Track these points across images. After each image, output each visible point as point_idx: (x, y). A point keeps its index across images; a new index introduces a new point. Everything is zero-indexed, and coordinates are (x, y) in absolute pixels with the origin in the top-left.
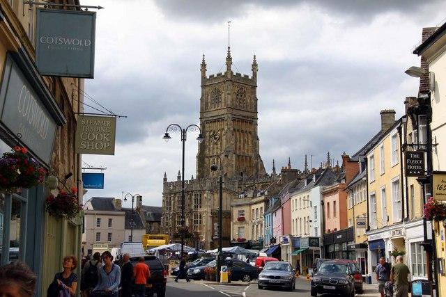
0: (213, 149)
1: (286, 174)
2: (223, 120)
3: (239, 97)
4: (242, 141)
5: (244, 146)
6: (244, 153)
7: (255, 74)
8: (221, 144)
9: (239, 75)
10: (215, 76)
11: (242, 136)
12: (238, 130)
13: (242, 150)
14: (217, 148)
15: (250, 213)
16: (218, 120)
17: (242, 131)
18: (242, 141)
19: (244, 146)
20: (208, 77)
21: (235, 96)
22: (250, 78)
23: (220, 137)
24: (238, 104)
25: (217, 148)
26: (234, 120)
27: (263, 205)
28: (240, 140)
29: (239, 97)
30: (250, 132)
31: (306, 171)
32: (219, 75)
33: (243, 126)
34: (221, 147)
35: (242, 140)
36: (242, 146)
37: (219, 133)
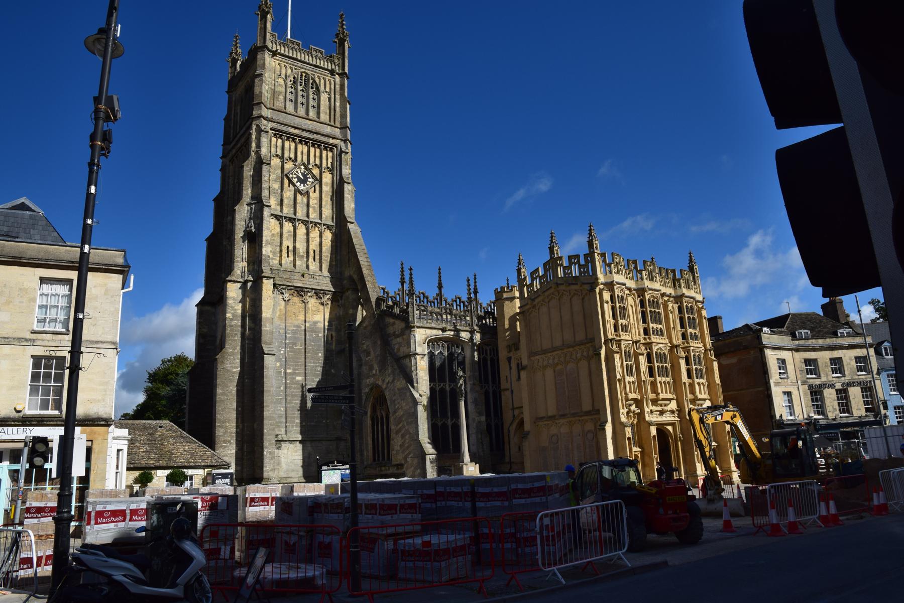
16: (316, 144)
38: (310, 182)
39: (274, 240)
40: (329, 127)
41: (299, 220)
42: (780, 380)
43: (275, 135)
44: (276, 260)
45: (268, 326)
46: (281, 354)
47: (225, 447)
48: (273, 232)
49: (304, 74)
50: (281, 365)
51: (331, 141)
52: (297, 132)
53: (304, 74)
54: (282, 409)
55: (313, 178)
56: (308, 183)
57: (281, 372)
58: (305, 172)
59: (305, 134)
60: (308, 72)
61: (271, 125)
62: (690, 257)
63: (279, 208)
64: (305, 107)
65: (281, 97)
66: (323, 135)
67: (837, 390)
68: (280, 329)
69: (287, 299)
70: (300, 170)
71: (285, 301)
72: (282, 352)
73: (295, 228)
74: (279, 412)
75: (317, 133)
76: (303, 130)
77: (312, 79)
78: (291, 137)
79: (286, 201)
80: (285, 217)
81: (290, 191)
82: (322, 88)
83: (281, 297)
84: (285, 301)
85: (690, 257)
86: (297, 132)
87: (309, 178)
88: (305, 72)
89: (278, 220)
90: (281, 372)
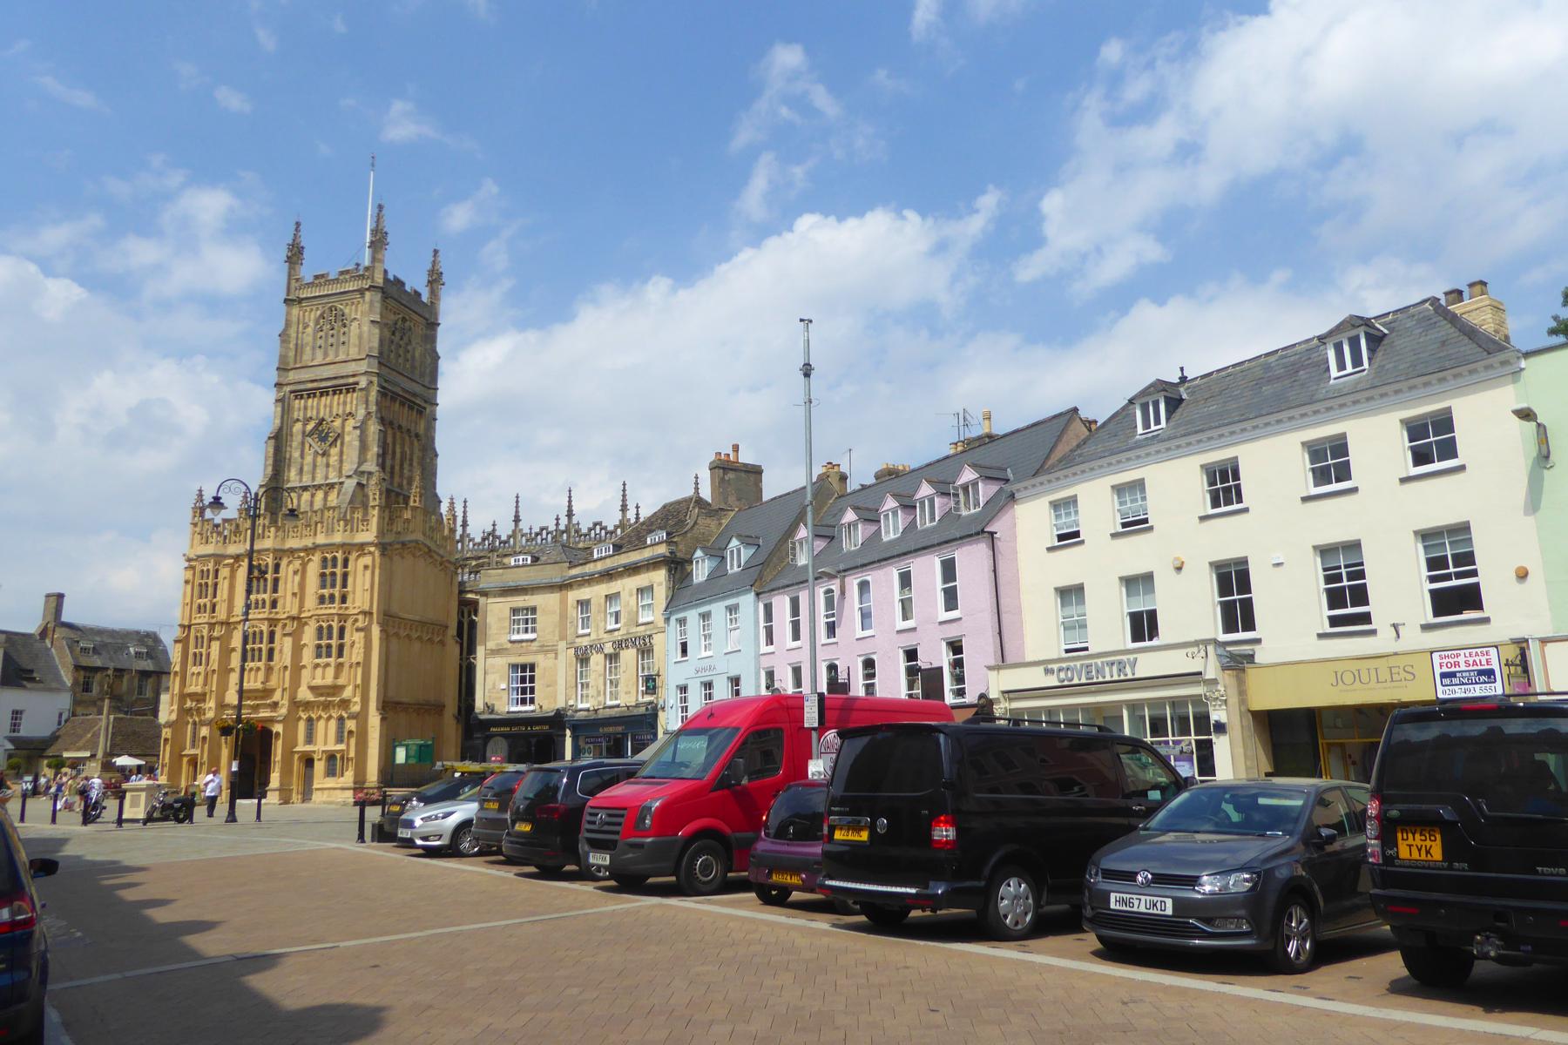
0: (315, 466)
1: (731, 475)
2: (351, 388)
3: (397, 338)
4: (398, 455)
5: (402, 466)
6: (400, 486)
7: (434, 294)
8: (341, 453)
9: (399, 283)
11: (398, 441)
12: (391, 423)
13: (397, 479)
14: (328, 465)
15: (563, 616)
16: (337, 390)
17: (400, 427)
18: (398, 455)
19: (402, 466)
20: (308, 279)
21: (387, 334)
22: (425, 298)
23: (339, 436)
24: (392, 355)
25: (328, 465)
26: (384, 393)
27: (659, 577)
28: (394, 453)
29: (397, 338)
30: (417, 436)
31: (622, 525)
33: (404, 417)
34: (341, 461)
35: (398, 450)
36: (397, 468)
37: (338, 423)
40: (354, 363)
41: (314, 486)
42: (509, 645)
43: (296, 397)
49: (333, 309)
51: (351, 380)
53: (333, 309)
56: (330, 439)
63: (298, 478)
64: (322, 350)
65: (308, 348)
66: (342, 377)
67: (606, 655)
73: (313, 496)
75: (335, 378)
76: (322, 380)
77: (341, 310)
78: (311, 394)
79: (305, 468)
80: (301, 487)
81: (310, 454)
86: (315, 385)
88: (332, 306)
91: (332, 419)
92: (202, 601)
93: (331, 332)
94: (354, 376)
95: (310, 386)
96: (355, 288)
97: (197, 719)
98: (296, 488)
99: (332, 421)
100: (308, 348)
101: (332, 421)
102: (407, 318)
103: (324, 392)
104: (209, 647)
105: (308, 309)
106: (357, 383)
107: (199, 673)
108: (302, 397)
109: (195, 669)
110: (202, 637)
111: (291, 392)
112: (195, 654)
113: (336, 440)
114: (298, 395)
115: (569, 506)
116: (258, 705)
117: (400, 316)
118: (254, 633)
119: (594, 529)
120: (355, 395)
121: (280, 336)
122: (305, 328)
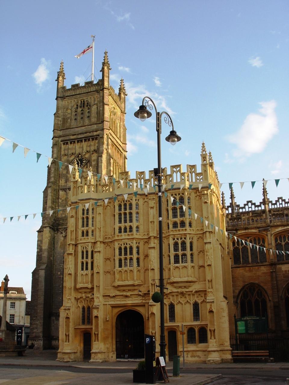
10: (82, 84)
16: (87, 139)
20: (69, 87)
32: (89, 84)
38: (84, 163)
39: (63, 203)
40: (95, 125)
43: (64, 144)
44: (64, 214)
45: (45, 254)
46: (61, 267)
47: (35, 319)
48: (63, 199)
49: (82, 101)
50: (61, 273)
51: (95, 134)
52: (75, 137)
53: (82, 101)
54: (61, 298)
55: (86, 160)
56: (83, 164)
57: (61, 277)
58: (81, 158)
59: (80, 136)
60: (84, 98)
61: (60, 139)
62: (203, 147)
68: (61, 253)
69: (64, 236)
70: (79, 158)
71: (63, 237)
72: (61, 266)
74: (59, 300)
78: (73, 142)
82: (93, 103)
83: (61, 235)
84: (63, 237)
85: (203, 147)
86: (75, 137)
87: (84, 160)
88: (82, 100)
89: (65, 191)
90: (61, 277)
91: (85, 154)
92: (85, 229)
93: (82, 112)
94: (96, 131)
95: (72, 137)
96: (94, 90)
97: (85, 306)
98: (66, 189)
99: (85, 155)
100: (69, 120)
101: (85, 155)
102: (115, 108)
103: (80, 141)
104: (92, 257)
105: (69, 101)
106: (99, 135)
107: (87, 274)
108: (67, 143)
109: (85, 272)
110: (87, 252)
111: (61, 141)
112: (83, 263)
113: (87, 164)
114: (65, 143)
115: (231, 193)
116: (131, 295)
117: (113, 106)
118: (126, 248)
119: (247, 204)
120: (97, 141)
121: (54, 115)
122: (67, 110)
